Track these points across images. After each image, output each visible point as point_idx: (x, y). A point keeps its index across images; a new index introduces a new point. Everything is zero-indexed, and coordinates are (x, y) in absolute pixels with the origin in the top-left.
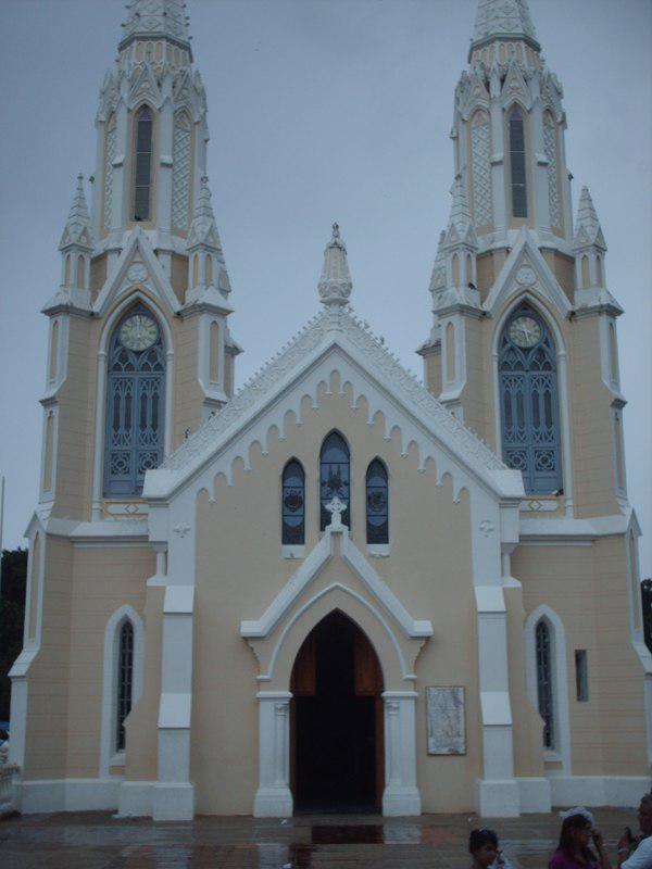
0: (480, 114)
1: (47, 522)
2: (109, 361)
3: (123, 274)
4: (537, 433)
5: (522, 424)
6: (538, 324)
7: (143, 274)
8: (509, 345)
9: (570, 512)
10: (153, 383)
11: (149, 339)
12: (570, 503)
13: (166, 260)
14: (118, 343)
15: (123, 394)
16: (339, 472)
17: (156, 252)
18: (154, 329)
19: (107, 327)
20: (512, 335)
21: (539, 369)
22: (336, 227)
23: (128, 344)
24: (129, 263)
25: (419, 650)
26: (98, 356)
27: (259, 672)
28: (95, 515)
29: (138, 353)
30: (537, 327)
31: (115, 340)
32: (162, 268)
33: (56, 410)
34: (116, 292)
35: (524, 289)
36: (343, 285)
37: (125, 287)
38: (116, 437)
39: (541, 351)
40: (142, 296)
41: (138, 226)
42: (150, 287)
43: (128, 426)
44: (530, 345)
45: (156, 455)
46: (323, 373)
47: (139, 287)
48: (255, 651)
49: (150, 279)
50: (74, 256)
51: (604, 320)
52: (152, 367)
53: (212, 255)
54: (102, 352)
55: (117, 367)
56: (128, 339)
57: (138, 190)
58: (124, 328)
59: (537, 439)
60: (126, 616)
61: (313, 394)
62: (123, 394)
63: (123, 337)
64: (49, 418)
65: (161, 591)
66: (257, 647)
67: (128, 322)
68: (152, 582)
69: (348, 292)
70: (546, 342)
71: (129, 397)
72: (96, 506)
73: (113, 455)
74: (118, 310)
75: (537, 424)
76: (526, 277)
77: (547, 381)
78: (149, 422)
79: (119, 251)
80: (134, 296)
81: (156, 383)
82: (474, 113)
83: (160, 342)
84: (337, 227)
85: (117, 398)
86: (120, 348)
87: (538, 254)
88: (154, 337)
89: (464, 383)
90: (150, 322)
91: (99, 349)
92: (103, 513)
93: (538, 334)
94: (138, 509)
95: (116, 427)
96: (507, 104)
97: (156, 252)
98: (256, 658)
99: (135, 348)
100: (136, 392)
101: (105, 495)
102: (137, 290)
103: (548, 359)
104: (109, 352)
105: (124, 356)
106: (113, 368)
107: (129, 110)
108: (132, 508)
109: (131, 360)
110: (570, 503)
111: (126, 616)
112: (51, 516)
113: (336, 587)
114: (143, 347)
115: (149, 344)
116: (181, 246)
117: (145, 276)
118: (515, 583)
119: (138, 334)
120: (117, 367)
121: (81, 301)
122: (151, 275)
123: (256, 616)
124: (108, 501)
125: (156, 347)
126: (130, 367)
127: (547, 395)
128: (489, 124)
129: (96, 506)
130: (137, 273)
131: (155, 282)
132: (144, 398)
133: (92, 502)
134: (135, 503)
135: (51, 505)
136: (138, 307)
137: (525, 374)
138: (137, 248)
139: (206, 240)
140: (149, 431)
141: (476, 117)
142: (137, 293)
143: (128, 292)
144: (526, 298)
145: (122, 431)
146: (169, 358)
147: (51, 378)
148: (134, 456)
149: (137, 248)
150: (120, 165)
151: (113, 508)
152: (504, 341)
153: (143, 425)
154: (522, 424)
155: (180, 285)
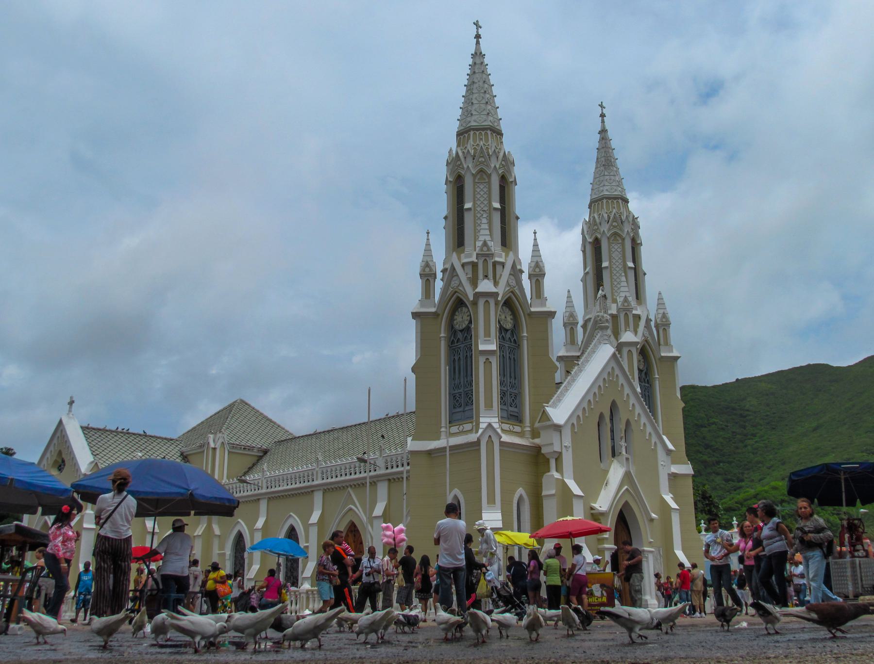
13: (469, 269)
15: (457, 358)
17: (463, 265)
26: (440, 338)
28: (443, 435)
29: (461, 331)
31: (451, 327)
40: (460, 296)
42: (461, 288)
47: (456, 290)
53: (487, 259)
55: (453, 342)
58: (455, 317)
62: (457, 358)
67: (457, 313)
73: (454, 397)
80: (455, 296)
83: (470, 322)
88: (469, 318)
91: (440, 333)
99: (461, 328)
101: (450, 422)
102: (456, 292)
109: (459, 337)
114: (464, 326)
115: (467, 323)
116: (474, 259)
119: (461, 321)
133: (441, 427)
139: (482, 250)
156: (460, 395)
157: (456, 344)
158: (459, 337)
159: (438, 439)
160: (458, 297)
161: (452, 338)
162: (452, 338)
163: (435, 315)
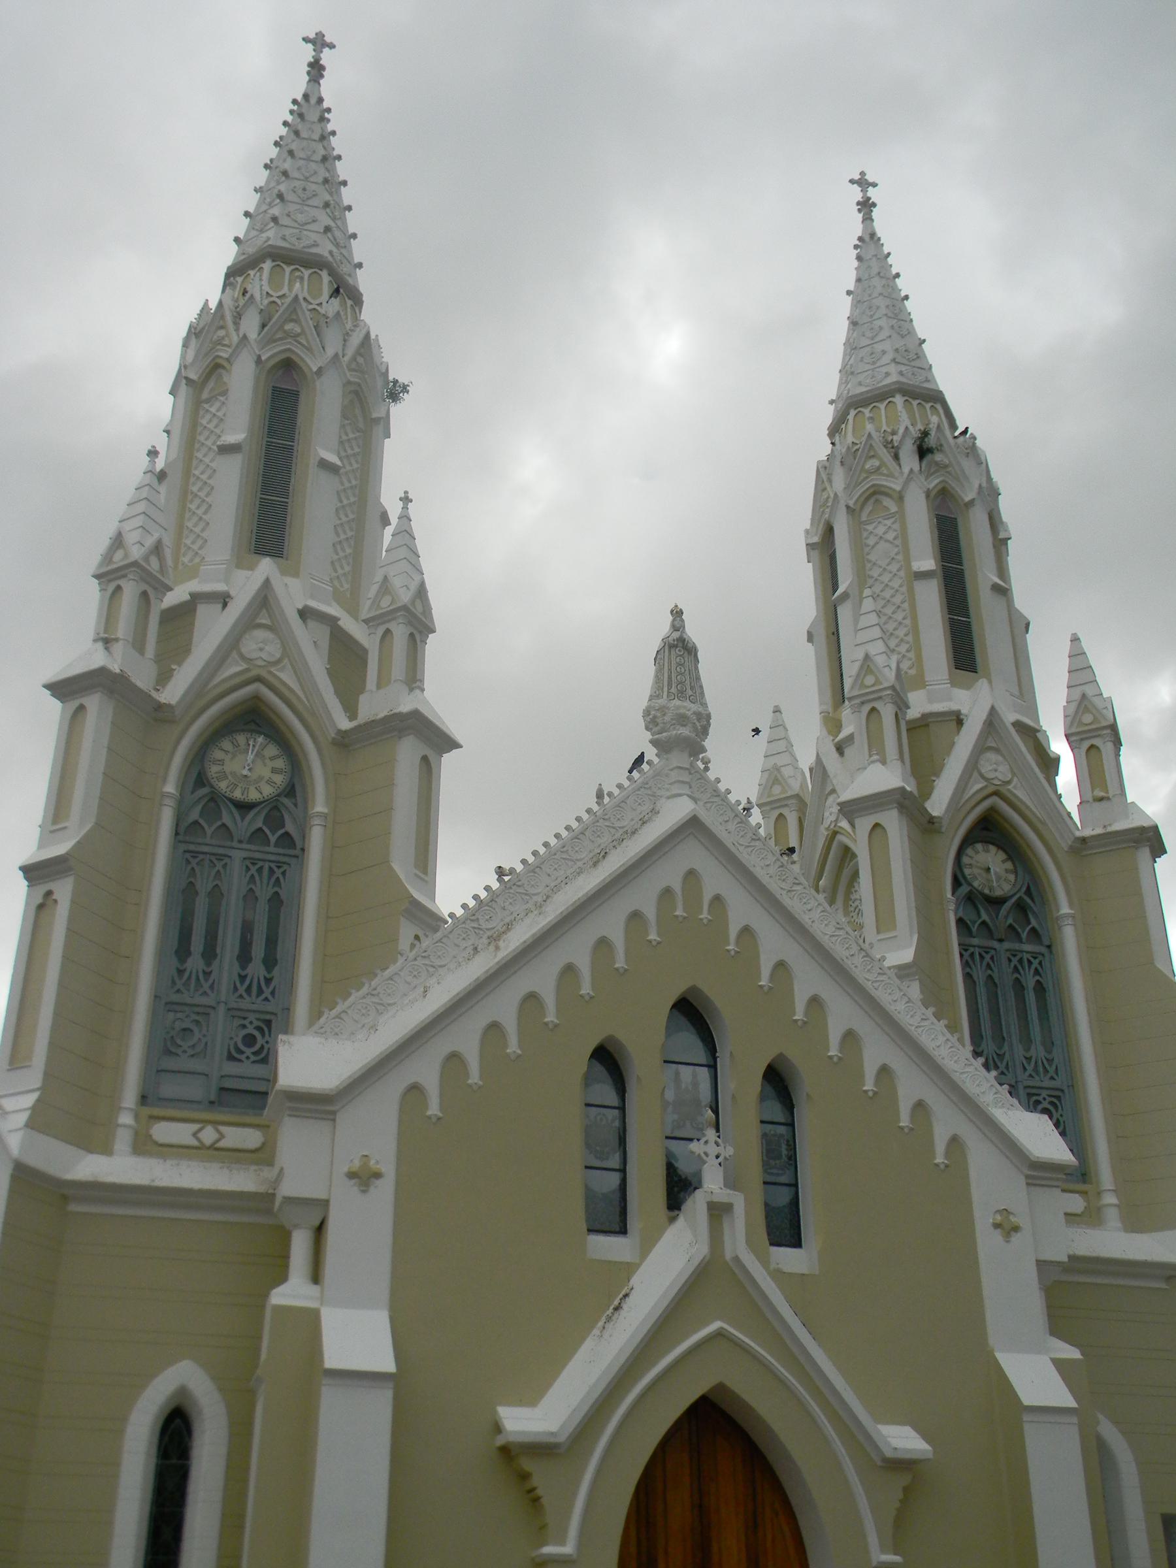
0: (877, 500)
1: (19, 1135)
3: (231, 645)
4: (1029, 1059)
5: (1000, 1039)
6: (1010, 858)
7: (273, 650)
8: (964, 889)
9: (1112, 1217)
10: (271, 871)
11: (270, 782)
12: (1110, 1199)
13: (323, 633)
14: (201, 780)
16: (695, 1084)
18: (280, 763)
19: (186, 743)
20: (967, 871)
21: (1021, 941)
22: (677, 613)
23: (223, 786)
24: (247, 624)
25: (901, 1495)
27: (541, 1533)
28: (123, 1140)
29: (244, 807)
30: (1009, 865)
33: (64, 890)
34: (213, 676)
35: (991, 789)
36: (699, 715)
37: (233, 668)
39: (1021, 908)
41: (266, 566)
42: (287, 677)
43: (210, 954)
44: (998, 893)
45: (268, 1023)
46: (669, 874)
47: (264, 674)
48: (536, 1481)
49: (286, 661)
50: (130, 590)
51: (1144, 853)
52: (273, 839)
54: (170, 788)
56: (223, 776)
57: (263, 504)
58: (218, 754)
59: (1030, 1068)
60: (183, 1391)
61: (650, 913)
62: (203, 886)
63: (213, 770)
64: (41, 907)
65: (310, 1321)
66: (542, 1477)
67: (226, 744)
68: (281, 1296)
69: (705, 731)
70: (1028, 892)
71: (216, 895)
72: (126, 1119)
75: (1027, 1041)
76: (995, 768)
77: (1035, 963)
78: (258, 950)
79: (224, 600)
81: (278, 873)
82: (867, 499)
84: (681, 613)
86: (204, 791)
87: (1012, 730)
88: (279, 779)
89: (916, 937)
90: (272, 750)
91: (164, 780)
92: (143, 1145)
93: (1012, 877)
94: (222, 1136)
95: (183, 951)
96: (934, 483)
97: (305, 614)
98: (534, 1500)
99: (237, 794)
100: (236, 882)
101: (144, 1099)
102: (258, 679)
103: (1034, 923)
105: (215, 801)
106: (184, 831)
107: (259, 361)
108: (209, 1135)
110: (1110, 1199)
111: (183, 1391)
112: (31, 1125)
113: (720, 1334)
114: (253, 796)
115: (268, 791)
117: (278, 655)
118: (1073, 1353)
121: (143, 677)
122: (290, 653)
123: (531, 1396)
124: (156, 1111)
125: (286, 801)
127: (1040, 988)
128: (901, 516)
129: (126, 1119)
132: (250, 897)
134: (215, 1123)
135: (29, 1100)
137: (995, 944)
140: (256, 969)
141: (869, 508)
143: (237, 680)
144: (992, 809)
145: (195, 963)
146: (316, 821)
147: (55, 822)
149: (264, 599)
150: (227, 450)
151: (164, 1132)
152: (957, 882)
153: (244, 957)
154: (1000, 1039)
157: (208, 840)
158: (226, 819)
159: (106, 1150)
160: (257, 698)
161: (195, 815)
162: (195, 815)
163: (160, 714)
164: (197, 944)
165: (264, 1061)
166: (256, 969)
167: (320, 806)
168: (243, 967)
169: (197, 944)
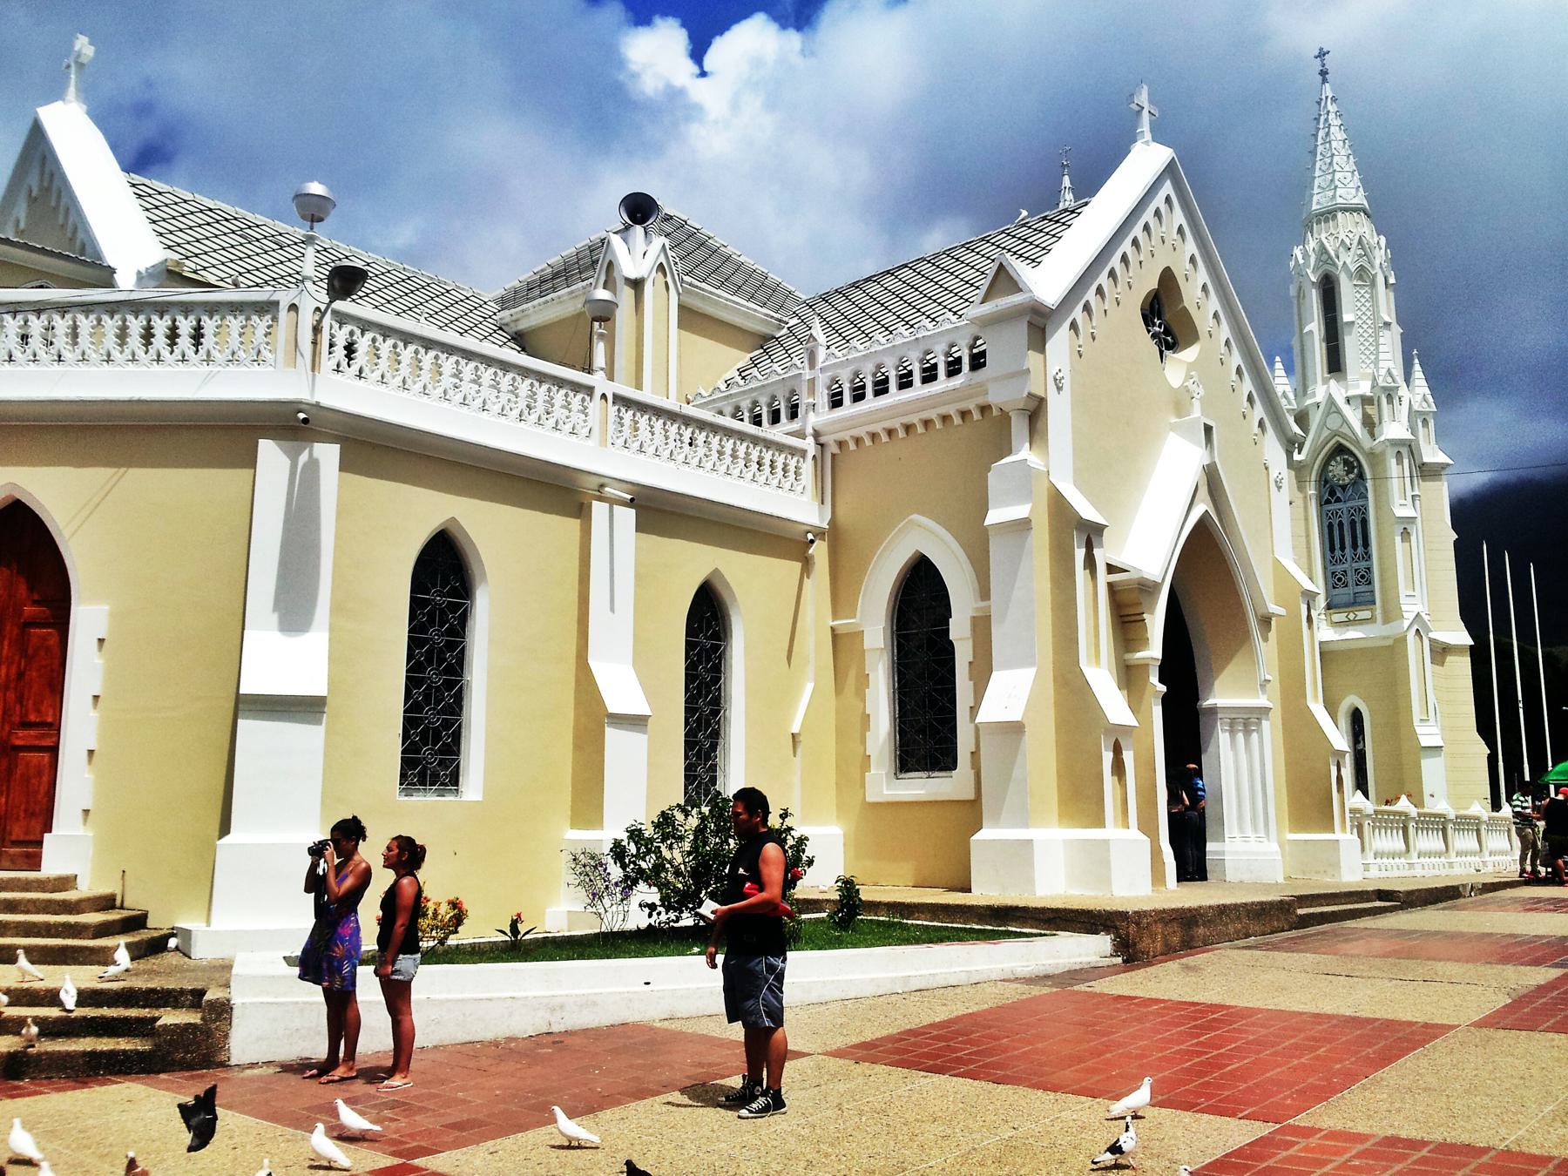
2: (1320, 497)
3: (1323, 425)
14: (1326, 482)
24: (1327, 414)
29: (1344, 487)
32: (1354, 417)
37: (1326, 433)
38: (1333, 558)
42: (1345, 430)
43: (1343, 548)
45: (1368, 569)
56: (1335, 476)
67: (1333, 463)
74: (1321, 457)
85: (1330, 526)
95: (1332, 549)
104: (1320, 492)
108: (1351, 616)
109: (1338, 494)
120: (1328, 502)
122: (1345, 421)
126: (1338, 500)
130: (1334, 423)
131: (1350, 427)
136: (1340, 450)
138: (1331, 402)
140: (1360, 550)
142: (1337, 438)
145: (1338, 553)
148: (1349, 573)
153: (1355, 546)
155: (1370, 424)
156: (1345, 571)
158: (1338, 494)
164: (1337, 546)
165: (1370, 583)
166: (1360, 550)
167: (1369, 484)
168: (1355, 550)
169: (1337, 546)
